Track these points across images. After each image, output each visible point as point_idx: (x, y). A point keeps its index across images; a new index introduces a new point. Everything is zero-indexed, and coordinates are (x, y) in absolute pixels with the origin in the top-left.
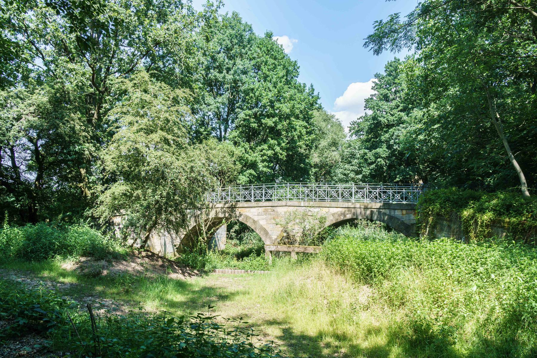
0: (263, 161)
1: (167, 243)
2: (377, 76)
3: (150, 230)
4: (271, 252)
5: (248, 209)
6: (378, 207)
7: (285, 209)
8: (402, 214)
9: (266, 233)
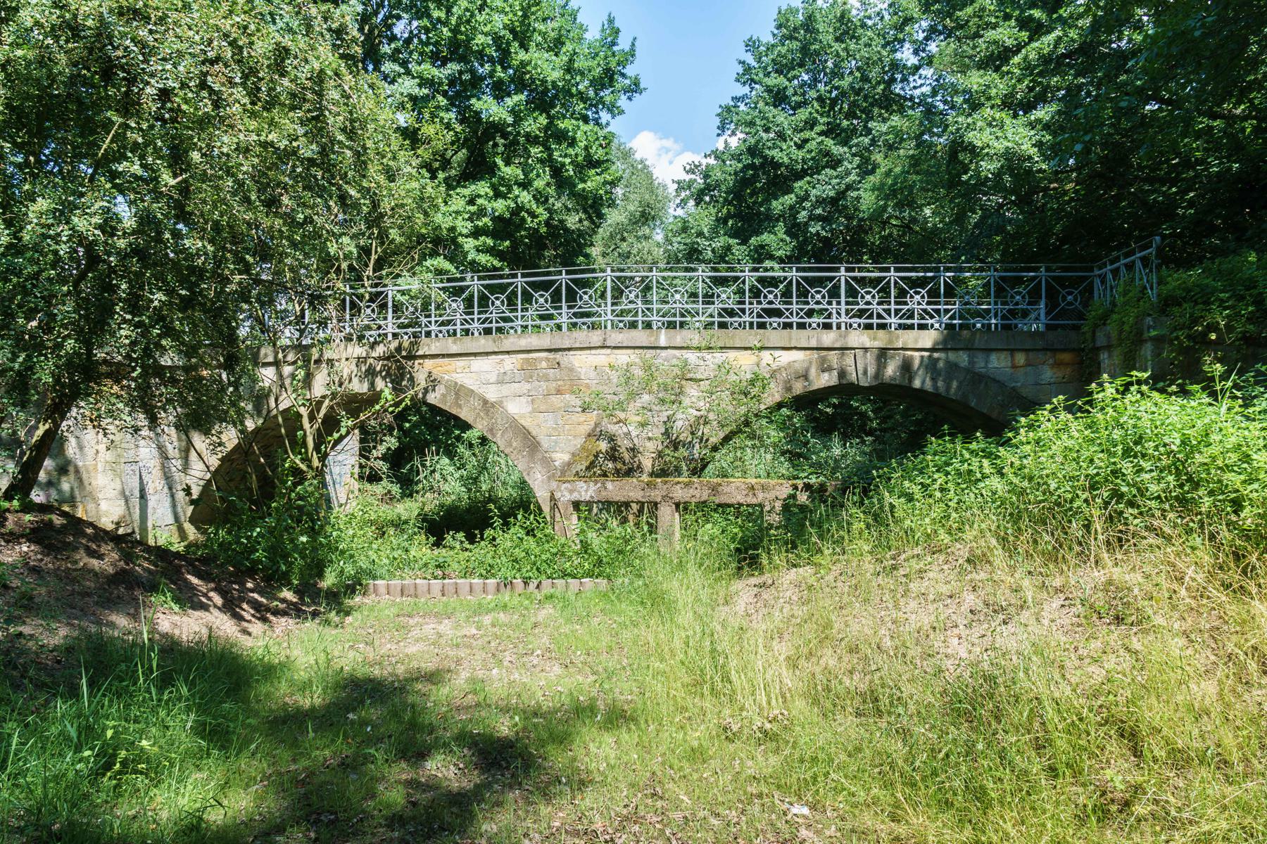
0: (476, 233)
1: (150, 489)
2: (752, 45)
3: (58, 411)
4: (576, 505)
5: (460, 363)
6: (929, 345)
7: (601, 358)
8: (1014, 367)
9: (532, 444)
